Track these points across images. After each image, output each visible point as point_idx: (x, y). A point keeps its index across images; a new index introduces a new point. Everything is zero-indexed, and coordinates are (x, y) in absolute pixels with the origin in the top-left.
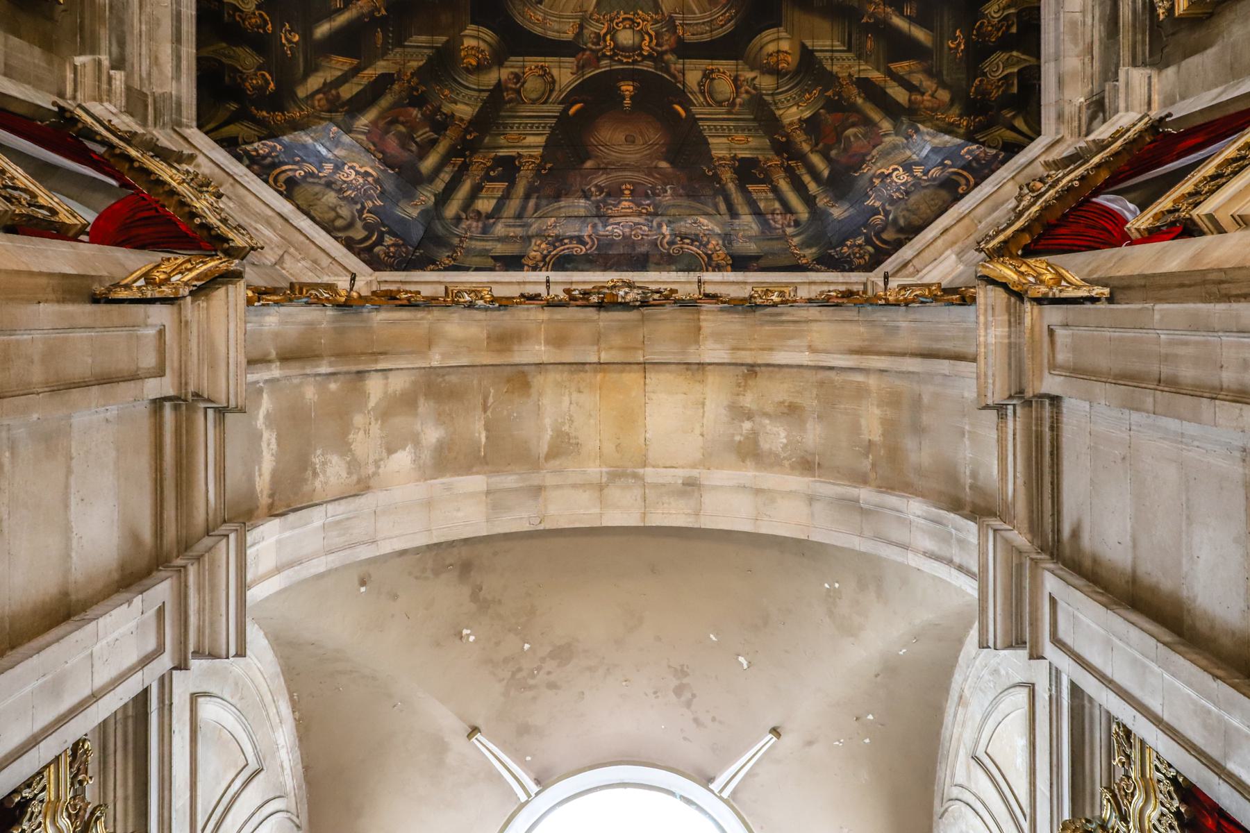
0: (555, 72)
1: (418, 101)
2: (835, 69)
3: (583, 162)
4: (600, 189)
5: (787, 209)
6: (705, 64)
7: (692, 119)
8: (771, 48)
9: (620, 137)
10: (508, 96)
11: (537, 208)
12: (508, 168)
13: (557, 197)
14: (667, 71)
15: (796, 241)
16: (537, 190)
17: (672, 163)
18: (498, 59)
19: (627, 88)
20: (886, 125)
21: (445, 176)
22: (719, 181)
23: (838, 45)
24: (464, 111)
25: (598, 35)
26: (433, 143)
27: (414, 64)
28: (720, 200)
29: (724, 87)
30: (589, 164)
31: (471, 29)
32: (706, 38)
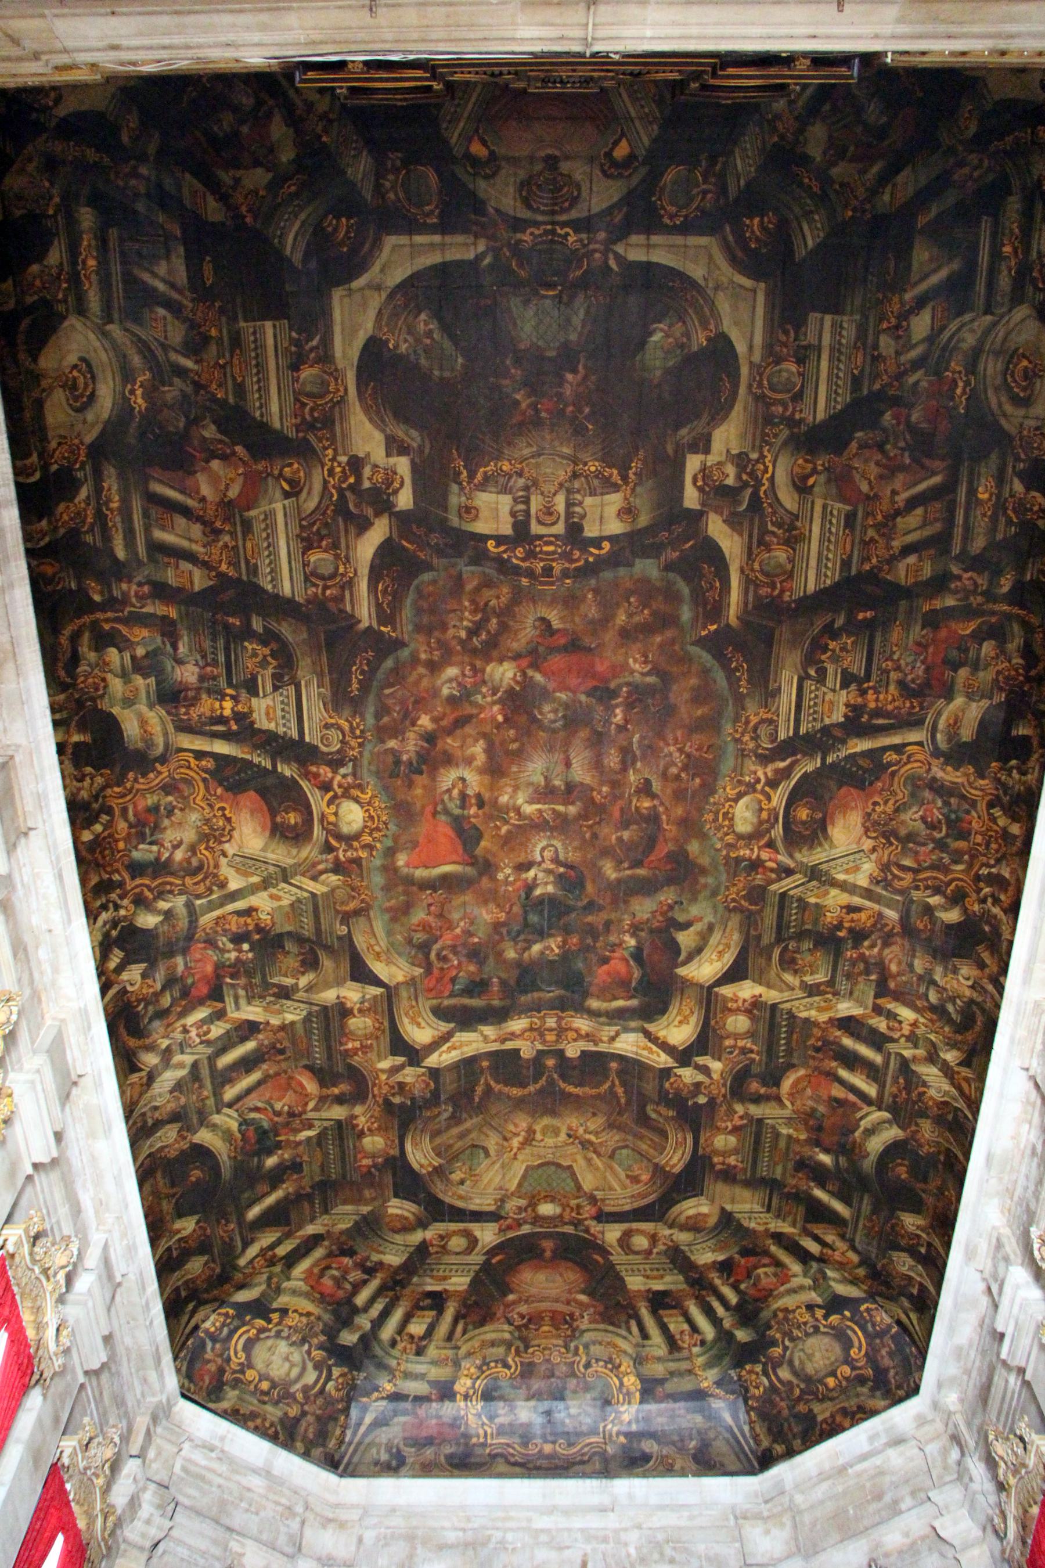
0: (478, 1234)
1: (351, 1253)
2: (753, 1225)
3: (505, 1295)
4: (522, 1317)
5: (695, 1329)
6: (625, 1226)
7: (612, 1266)
8: (691, 1212)
9: (541, 1277)
10: (432, 1250)
11: (464, 1332)
12: (437, 1301)
13: (482, 1323)
14: (587, 1230)
15: (700, 1361)
16: (464, 1317)
17: (591, 1294)
18: (422, 1224)
19: (548, 1245)
20: (796, 1267)
21: (378, 1307)
22: (634, 1308)
23: (757, 1208)
24: (394, 1259)
25: (520, 1208)
26: (365, 1282)
27: (343, 1226)
28: (633, 1324)
29: (641, 1242)
30: (511, 1297)
31: (394, 1202)
32: (627, 1208)
